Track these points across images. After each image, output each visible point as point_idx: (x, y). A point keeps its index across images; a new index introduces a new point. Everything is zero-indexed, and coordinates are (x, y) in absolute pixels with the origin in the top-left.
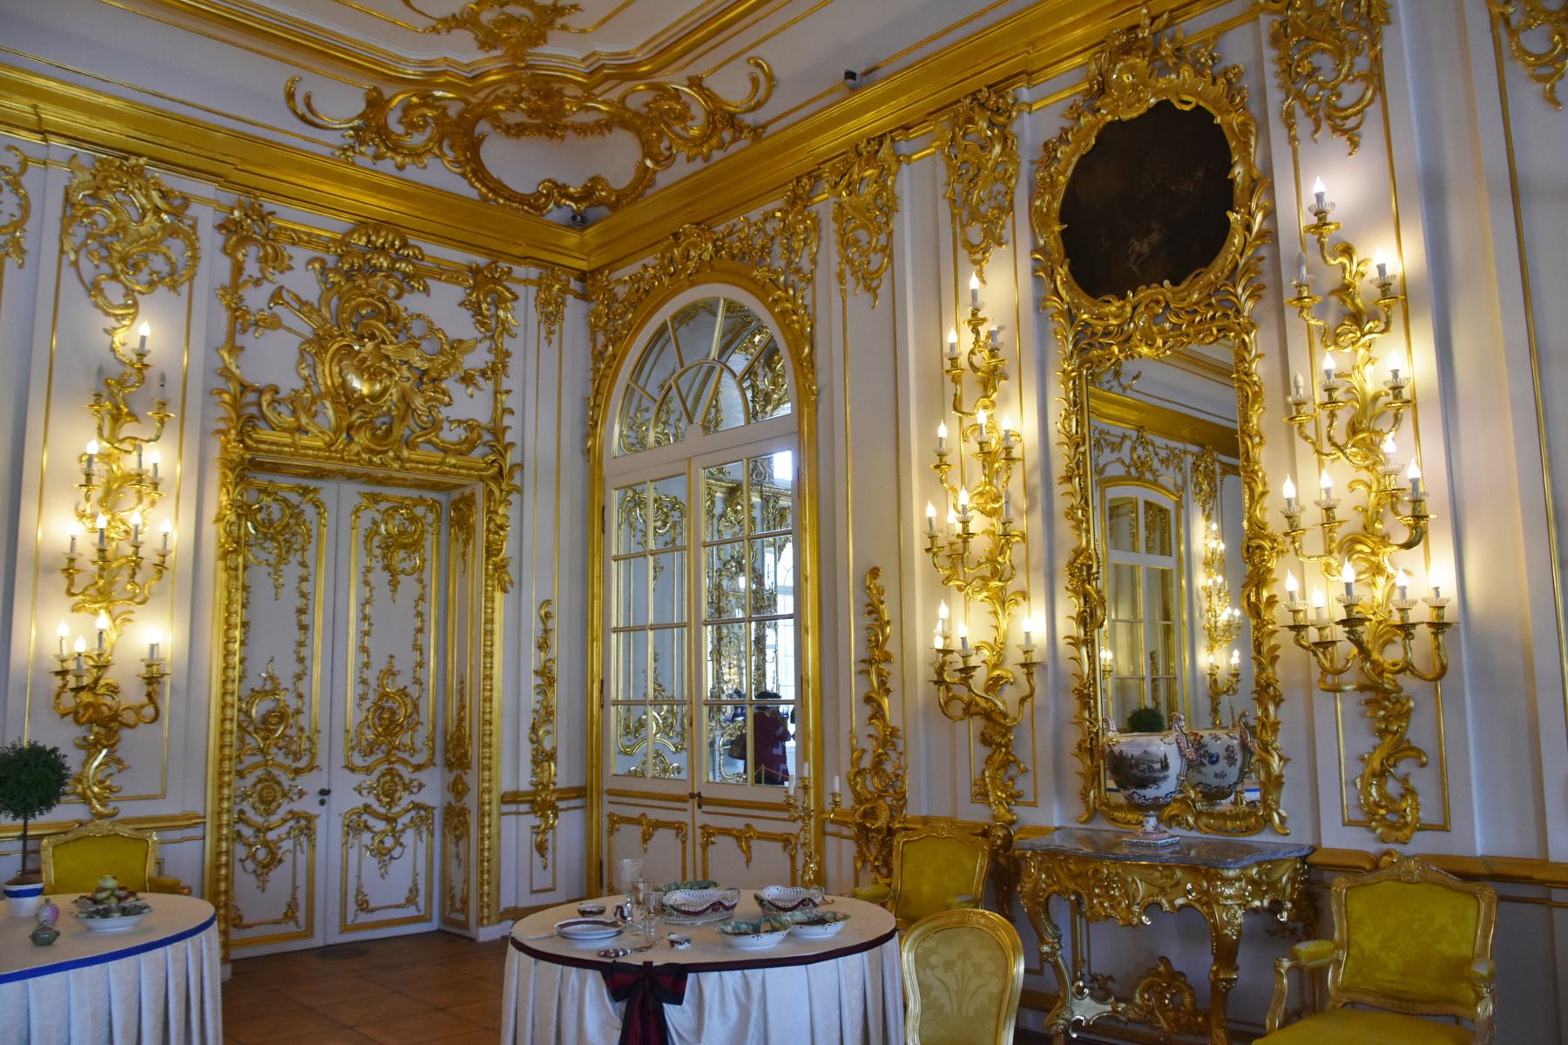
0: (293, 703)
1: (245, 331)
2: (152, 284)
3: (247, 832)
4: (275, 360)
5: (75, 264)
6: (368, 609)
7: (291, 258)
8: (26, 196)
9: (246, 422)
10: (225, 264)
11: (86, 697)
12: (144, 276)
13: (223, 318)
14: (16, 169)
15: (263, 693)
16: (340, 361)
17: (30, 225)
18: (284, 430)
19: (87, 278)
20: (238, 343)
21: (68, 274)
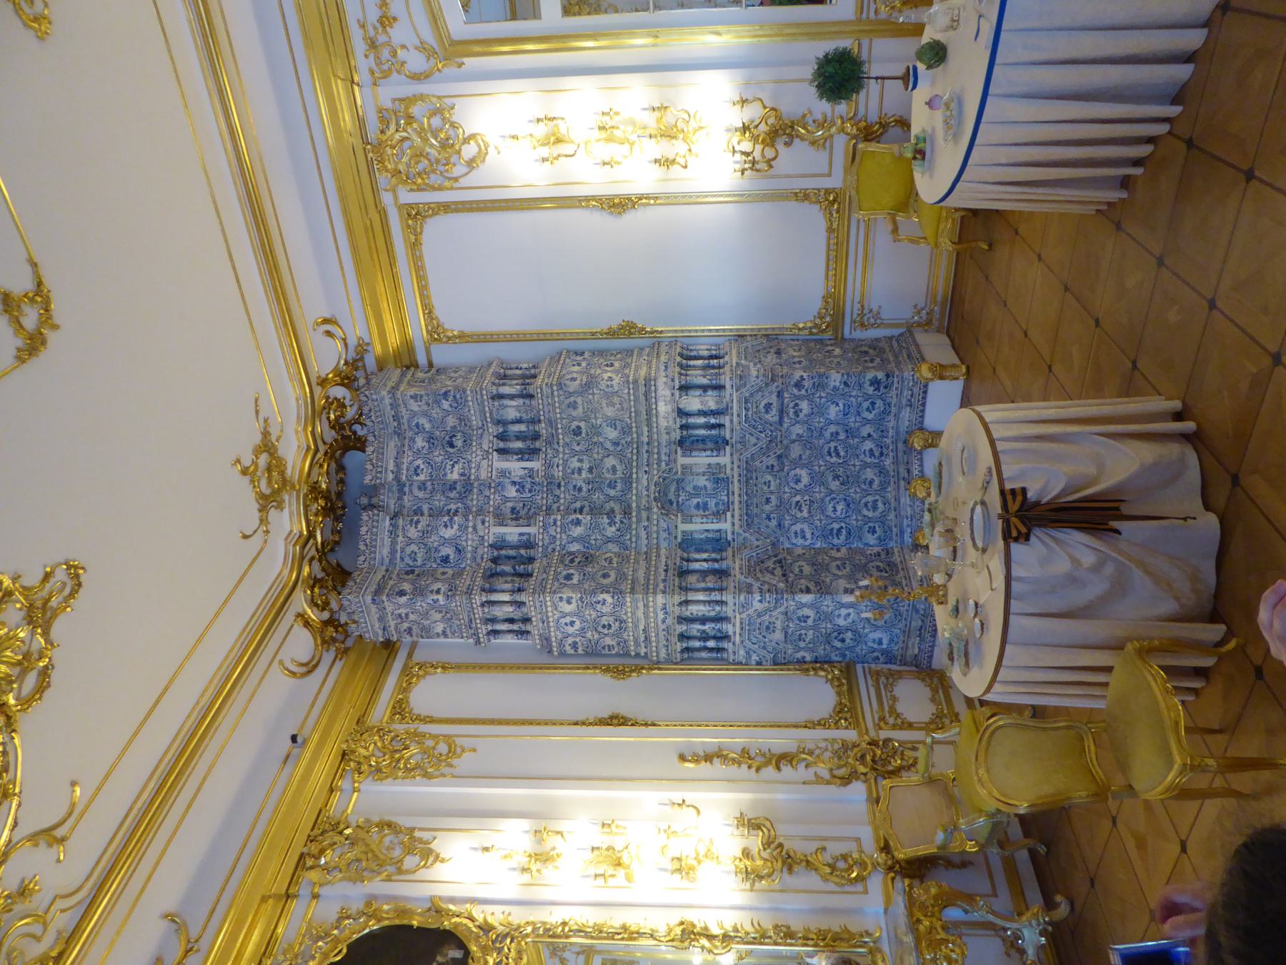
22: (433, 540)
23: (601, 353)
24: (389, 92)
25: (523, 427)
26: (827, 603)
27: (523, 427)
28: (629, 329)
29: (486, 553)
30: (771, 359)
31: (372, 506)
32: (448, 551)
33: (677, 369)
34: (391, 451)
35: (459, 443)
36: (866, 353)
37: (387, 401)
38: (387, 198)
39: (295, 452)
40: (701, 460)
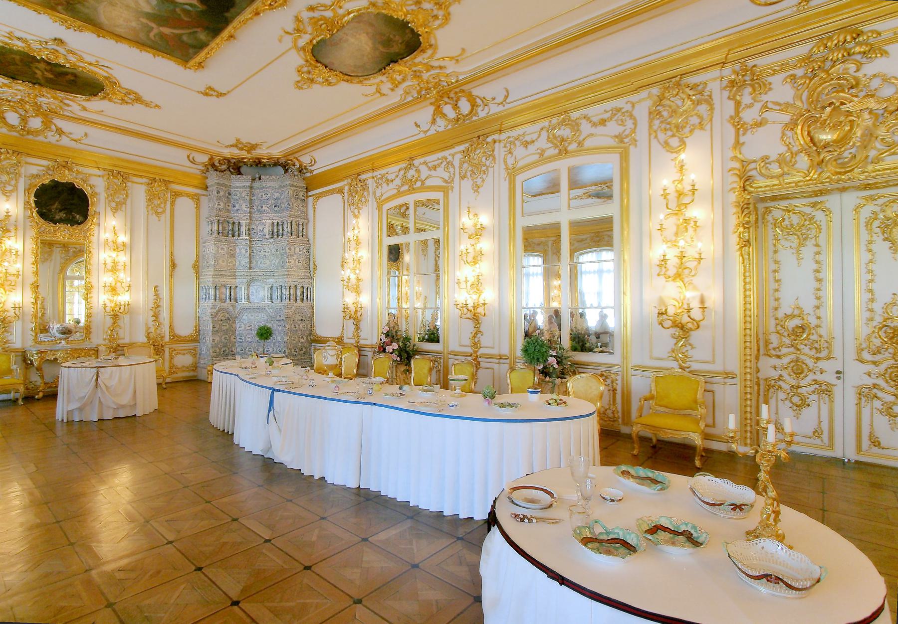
0: (813, 321)
1: (744, 134)
2: (691, 131)
3: (786, 387)
4: (766, 143)
5: (656, 137)
6: (870, 266)
7: (770, 84)
8: (635, 119)
9: (746, 180)
10: (732, 104)
11: (665, 316)
12: (687, 129)
13: (731, 131)
14: (630, 109)
15: (792, 316)
16: (809, 126)
17: (637, 130)
18: (772, 177)
19: (661, 141)
20: (741, 142)
21: (654, 142)
22: (241, 201)
23: (309, 258)
24: (371, 183)
25: (281, 231)
26: (210, 334)
27: (281, 231)
28: (315, 269)
29: (236, 221)
30: (298, 317)
31: (253, 180)
32: (237, 206)
33: (293, 286)
34: (273, 184)
35: (276, 209)
36: (301, 350)
37: (288, 183)
38: (345, 182)
39: (262, 152)
40: (267, 293)
